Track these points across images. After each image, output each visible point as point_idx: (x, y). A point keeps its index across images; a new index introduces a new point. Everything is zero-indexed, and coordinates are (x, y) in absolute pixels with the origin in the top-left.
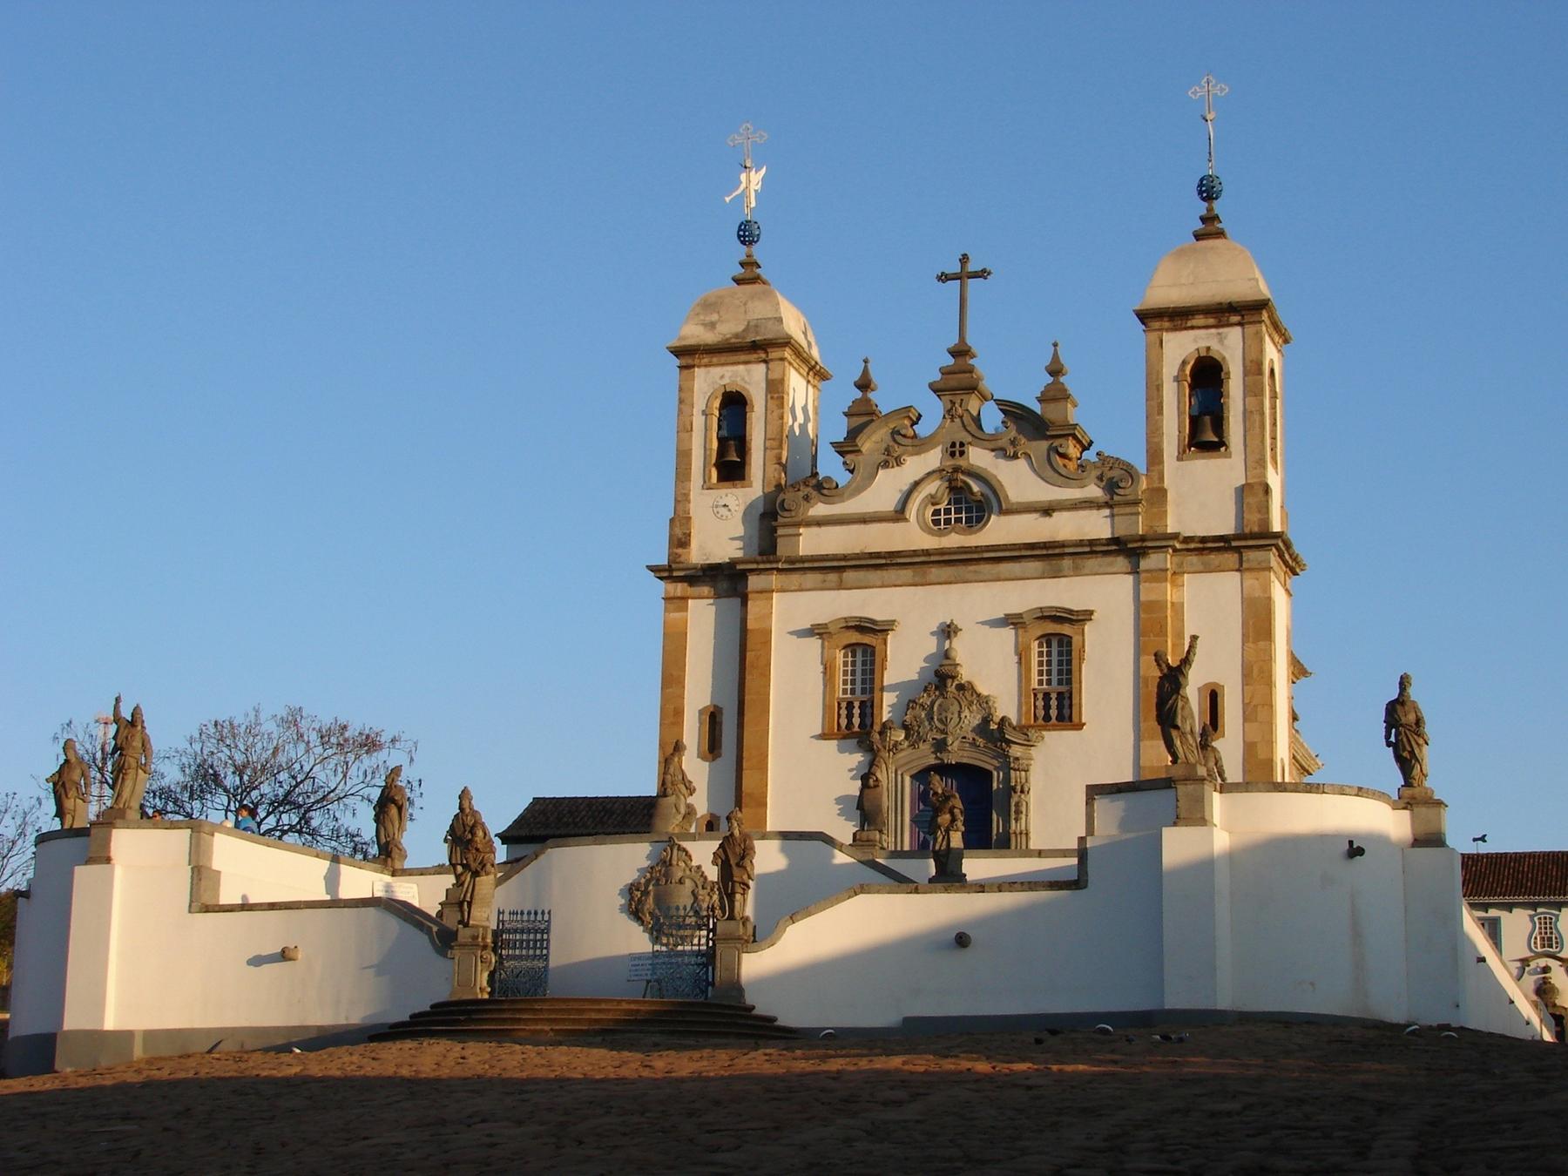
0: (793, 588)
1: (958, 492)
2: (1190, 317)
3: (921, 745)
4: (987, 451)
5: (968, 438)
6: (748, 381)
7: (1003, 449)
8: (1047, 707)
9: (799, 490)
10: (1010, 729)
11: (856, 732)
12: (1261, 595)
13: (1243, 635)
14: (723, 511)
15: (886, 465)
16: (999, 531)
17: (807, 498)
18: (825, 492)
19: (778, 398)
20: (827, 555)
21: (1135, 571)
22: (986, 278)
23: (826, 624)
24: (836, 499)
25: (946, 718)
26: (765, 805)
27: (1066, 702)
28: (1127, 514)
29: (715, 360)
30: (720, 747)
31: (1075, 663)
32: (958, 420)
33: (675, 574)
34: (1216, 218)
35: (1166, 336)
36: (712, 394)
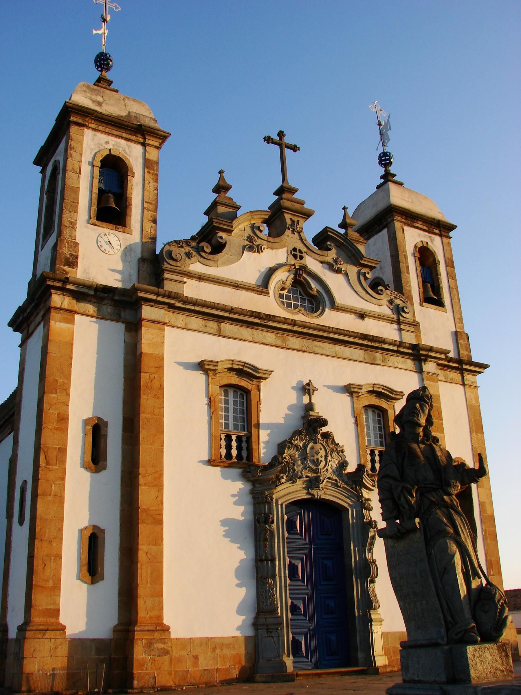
0: (180, 325)
2: (415, 221)
3: (298, 480)
4: (317, 262)
5: (304, 249)
6: (129, 154)
7: (328, 263)
9: (182, 247)
11: (234, 462)
13: (470, 428)
14: (107, 248)
15: (251, 249)
18: (203, 254)
19: (153, 174)
20: (218, 304)
23: (217, 362)
24: (211, 263)
25: (318, 459)
26: (160, 522)
29: (101, 128)
30: (105, 460)
32: (296, 234)
33: (69, 287)
35: (406, 228)
36: (99, 151)
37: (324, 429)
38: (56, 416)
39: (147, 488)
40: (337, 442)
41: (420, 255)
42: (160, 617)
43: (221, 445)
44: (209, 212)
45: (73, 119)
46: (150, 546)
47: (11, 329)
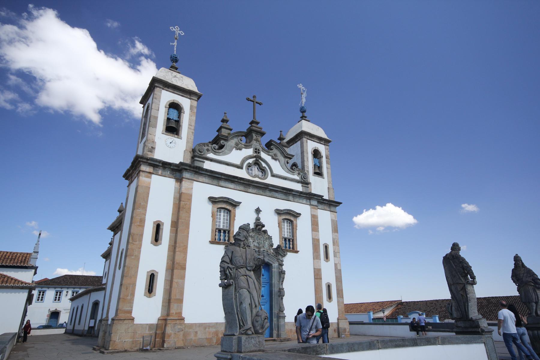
0: (201, 181)
1: (256, 163)
8: (286, 244)
10: (281, 250)
12: (335, 219)
16: (270, 180)
17: (208, 150)
19: (194, 112)
21: (310, 205)
22: (260, 105)
24: (217, 153)
25: (259, 242)
26: (184, 268)
27: (291, 243)
28: (306, 187)
31: (295, 230)
34: (306, 117)
35: (308, 141)
37: (264, 229)
38: (139, 219)
39: (179, 253)
40: (269, 235)
41: (314, 153)
42: (181, 313)
43: (216, 234)
44: (219, 130)
45: (156, 85)
46: (178, 280)
47: (124, 178)
